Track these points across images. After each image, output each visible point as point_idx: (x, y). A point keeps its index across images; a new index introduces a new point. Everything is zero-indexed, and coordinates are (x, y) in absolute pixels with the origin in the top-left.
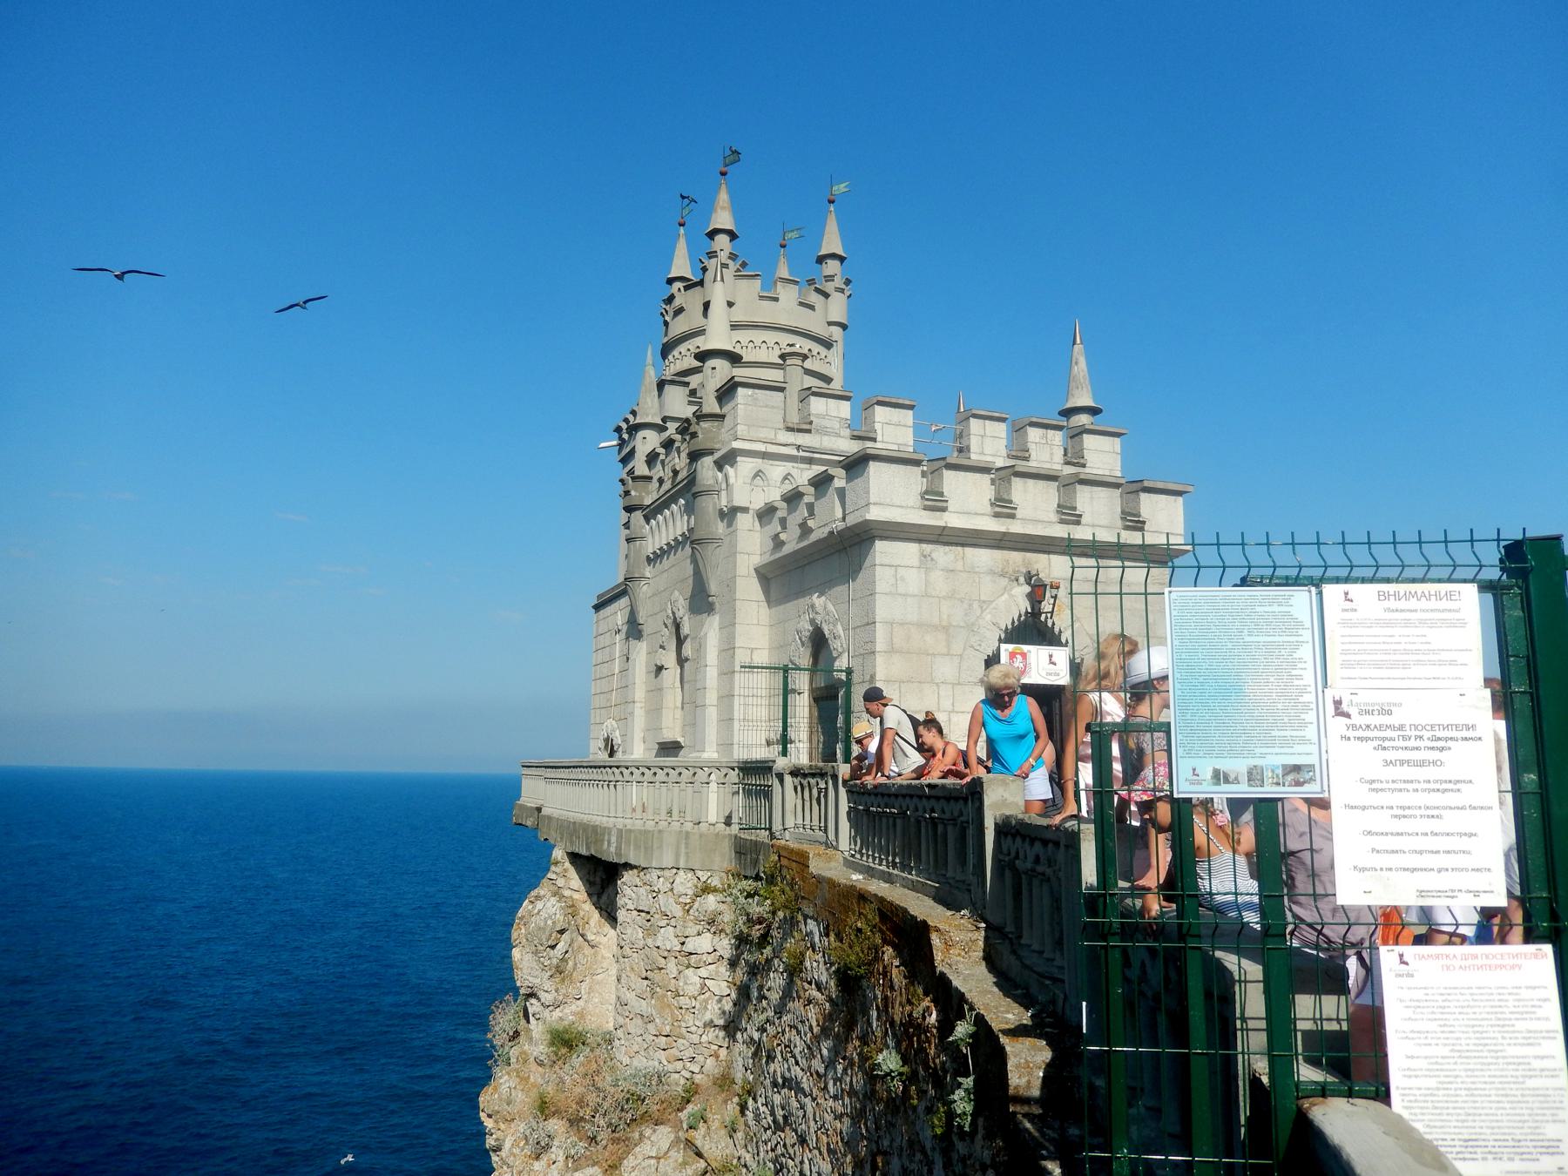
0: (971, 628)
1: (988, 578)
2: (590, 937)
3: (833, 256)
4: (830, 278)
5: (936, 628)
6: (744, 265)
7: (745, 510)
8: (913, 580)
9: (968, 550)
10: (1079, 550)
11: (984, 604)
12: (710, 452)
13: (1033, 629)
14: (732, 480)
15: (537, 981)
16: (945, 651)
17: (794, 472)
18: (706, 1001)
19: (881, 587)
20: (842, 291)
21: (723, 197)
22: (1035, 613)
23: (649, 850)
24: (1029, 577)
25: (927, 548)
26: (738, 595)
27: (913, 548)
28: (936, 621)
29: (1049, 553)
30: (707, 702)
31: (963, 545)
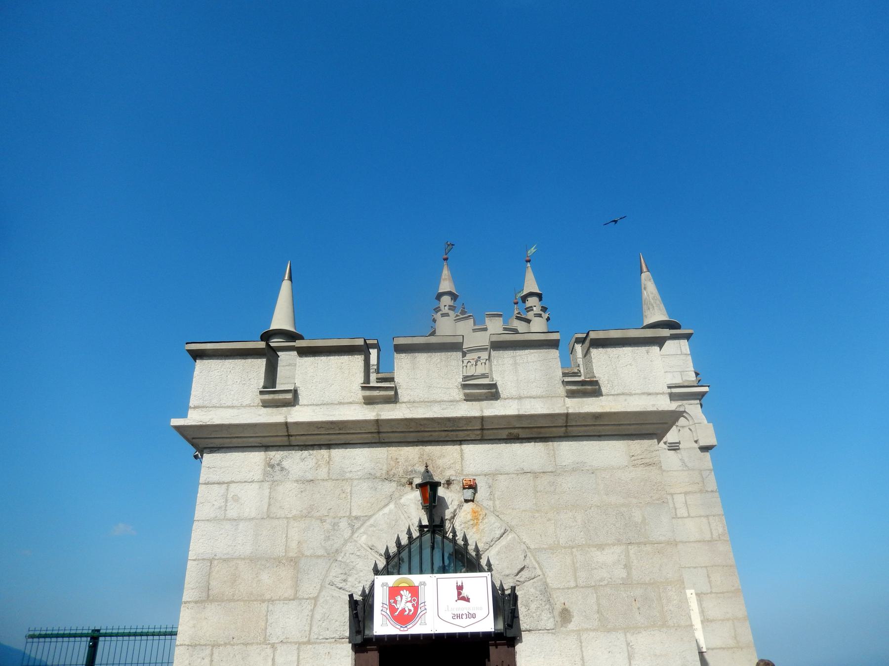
0: (332, 556)
1: (365, 485)
3: (531, 294)
4: (530, 309)
5: (278, 561)
6: (463, 312)
8: (251, 499)
10: (504, 434)
11: (356, 522)
13: (437, 546)
16: (290, 593)
19: (202, 510)
20: (540, 316)
21: (446, 272)
22: (436, 524)
25: (276, 455)
27: (256, 458)
28: (279, 551)
29: (461, 442)
31: (329, 446)
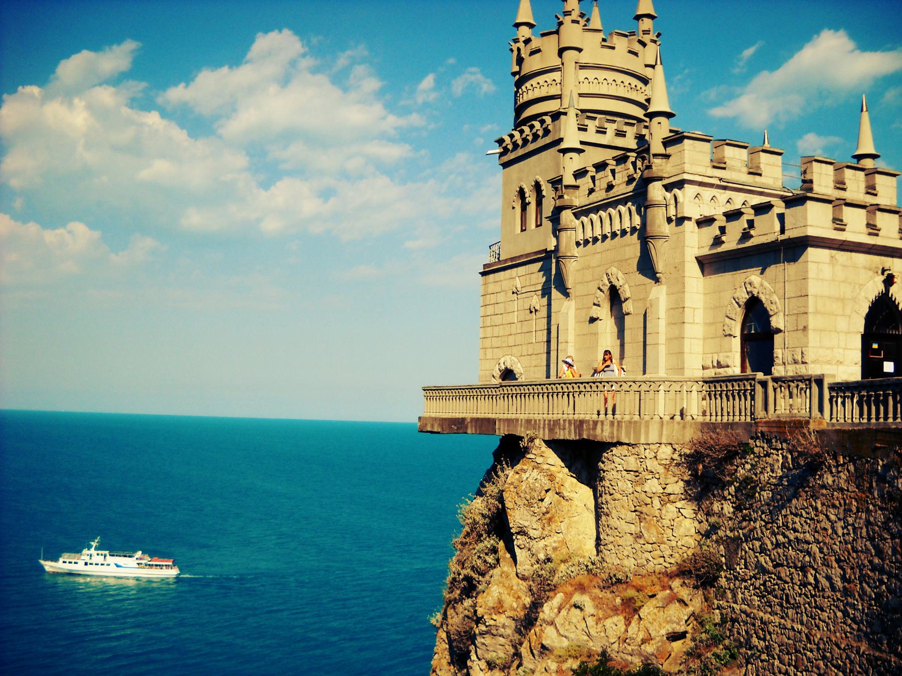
0: (854, 300)
2: (566, 494)
4: (646, 32)
7: (689, 219)
8: (827, 272)
9: (854, 254)
12: (660, 179)
14: (680, 199)
15: (526, 524)
17: (717, 195)
18: (681, 521)
20: (655, 42)
23: (637, 434)
24: (883, 271)
25: (834, 252)
26: (686, 274)
30: (660, 342)
